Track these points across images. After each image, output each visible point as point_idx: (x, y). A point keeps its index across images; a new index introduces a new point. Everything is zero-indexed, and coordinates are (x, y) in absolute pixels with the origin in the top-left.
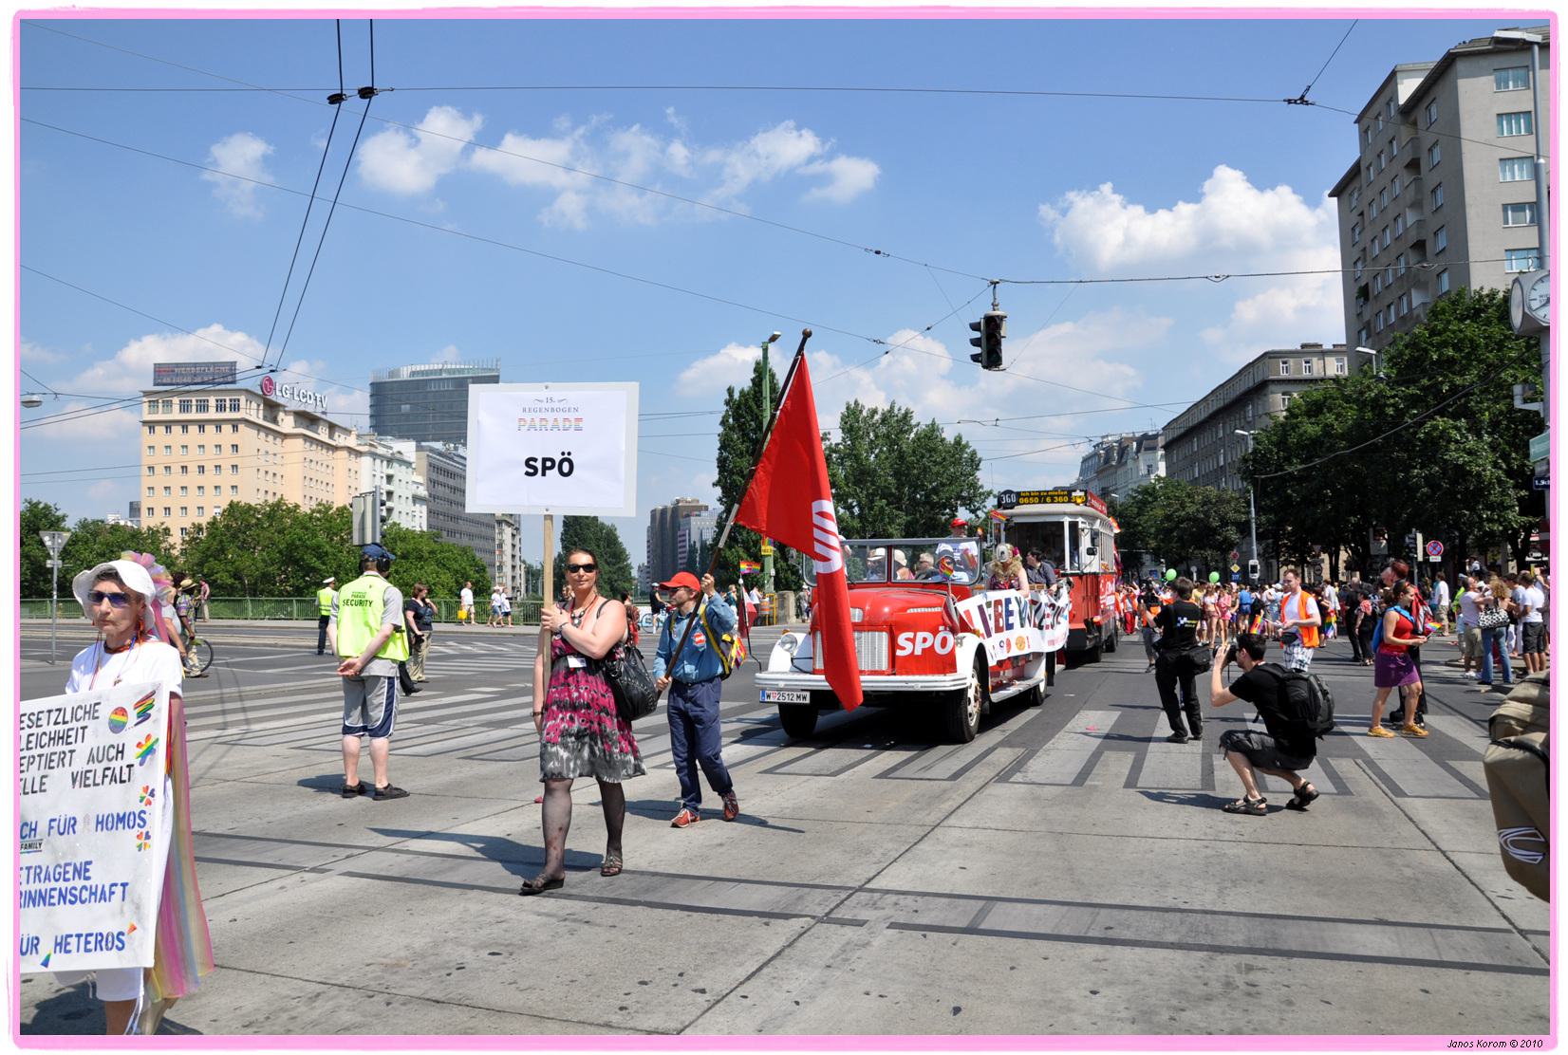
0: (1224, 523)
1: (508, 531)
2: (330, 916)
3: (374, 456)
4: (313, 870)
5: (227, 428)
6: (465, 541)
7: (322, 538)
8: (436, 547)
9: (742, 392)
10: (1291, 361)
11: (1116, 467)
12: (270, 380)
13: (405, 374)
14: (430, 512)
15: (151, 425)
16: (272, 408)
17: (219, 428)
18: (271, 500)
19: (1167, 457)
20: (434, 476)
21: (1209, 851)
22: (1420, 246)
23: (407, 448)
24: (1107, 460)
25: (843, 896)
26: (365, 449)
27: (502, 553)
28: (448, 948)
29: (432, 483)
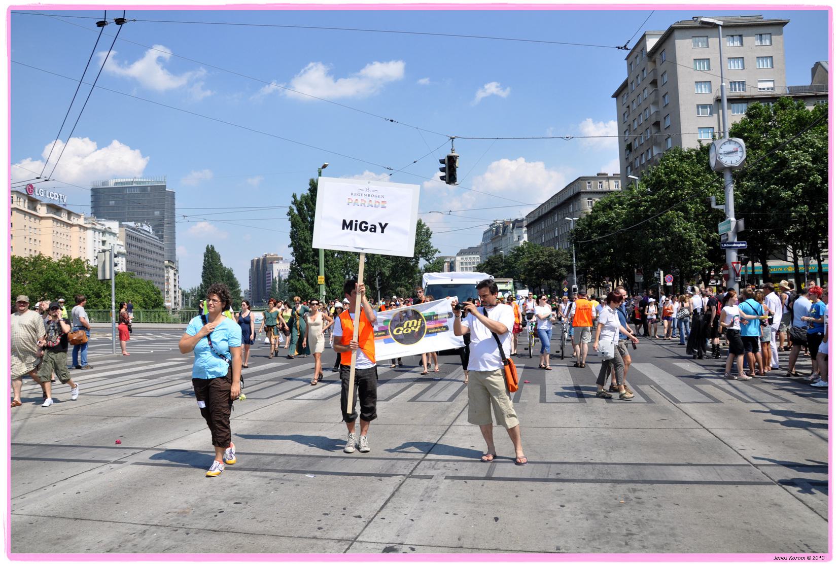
0: (560, 266)
1: (172, 272)
2: (133, 488)
3: (95, 230)
4: (115, 462)
6: (147, 278)
7: (65, 276)
8: (133, 281)
9: (302, 196)
10: (592, 182)
13: (111, 184)
14: (127, 261)
19: (528, 232)
20: (130, 241)
21: (594, 433)
22: (657, 124)
23: (114, 225)
24: (497, 233)
25: (416, 463)
26: (90, 226)
27: (168, 284)
28: (210, 501)
29: (128, 245)
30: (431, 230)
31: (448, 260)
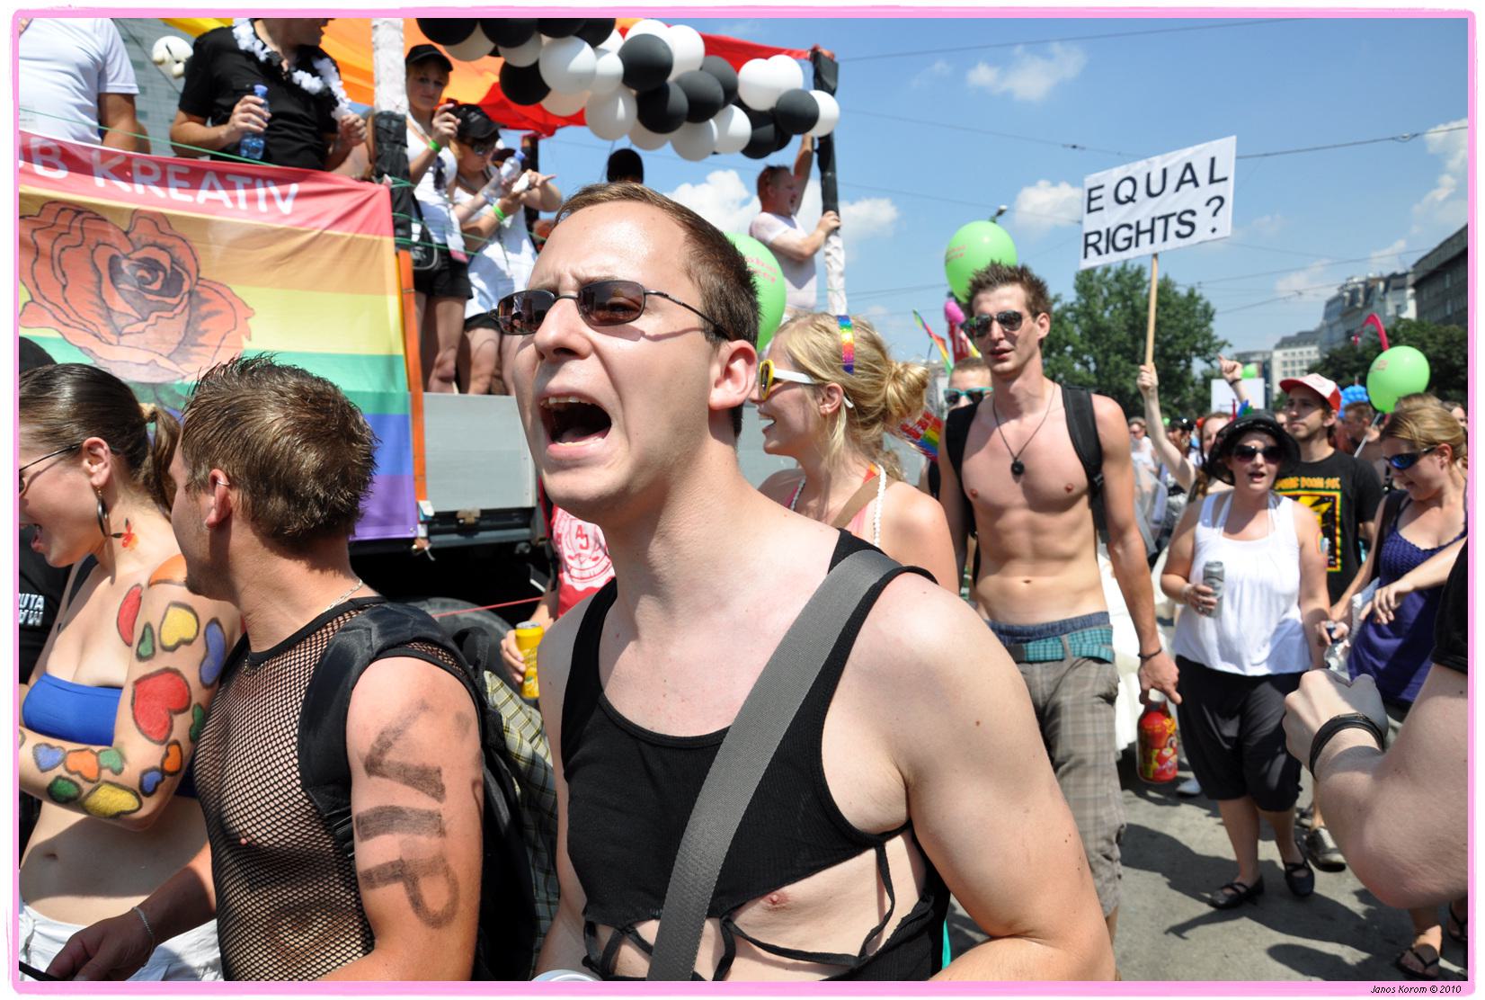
11: (1362, 310)
24: (1353, 300)
30: (1213, 305)
31: (1259, 358)
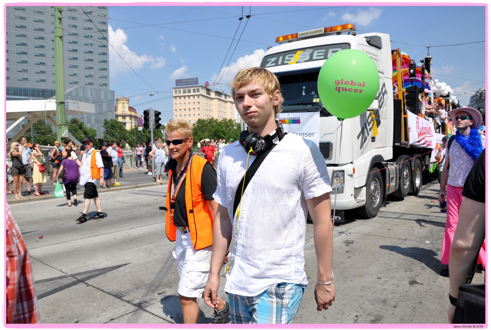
5: (196, 97)
7: (224, 128)
12: (207, 83)
15: (175, 97)
16: (208, 91)
17: (194, 97)
18: (211, 118)
